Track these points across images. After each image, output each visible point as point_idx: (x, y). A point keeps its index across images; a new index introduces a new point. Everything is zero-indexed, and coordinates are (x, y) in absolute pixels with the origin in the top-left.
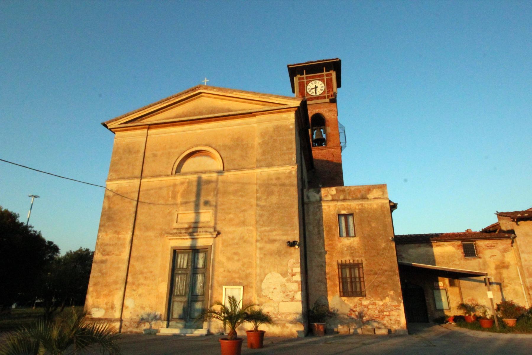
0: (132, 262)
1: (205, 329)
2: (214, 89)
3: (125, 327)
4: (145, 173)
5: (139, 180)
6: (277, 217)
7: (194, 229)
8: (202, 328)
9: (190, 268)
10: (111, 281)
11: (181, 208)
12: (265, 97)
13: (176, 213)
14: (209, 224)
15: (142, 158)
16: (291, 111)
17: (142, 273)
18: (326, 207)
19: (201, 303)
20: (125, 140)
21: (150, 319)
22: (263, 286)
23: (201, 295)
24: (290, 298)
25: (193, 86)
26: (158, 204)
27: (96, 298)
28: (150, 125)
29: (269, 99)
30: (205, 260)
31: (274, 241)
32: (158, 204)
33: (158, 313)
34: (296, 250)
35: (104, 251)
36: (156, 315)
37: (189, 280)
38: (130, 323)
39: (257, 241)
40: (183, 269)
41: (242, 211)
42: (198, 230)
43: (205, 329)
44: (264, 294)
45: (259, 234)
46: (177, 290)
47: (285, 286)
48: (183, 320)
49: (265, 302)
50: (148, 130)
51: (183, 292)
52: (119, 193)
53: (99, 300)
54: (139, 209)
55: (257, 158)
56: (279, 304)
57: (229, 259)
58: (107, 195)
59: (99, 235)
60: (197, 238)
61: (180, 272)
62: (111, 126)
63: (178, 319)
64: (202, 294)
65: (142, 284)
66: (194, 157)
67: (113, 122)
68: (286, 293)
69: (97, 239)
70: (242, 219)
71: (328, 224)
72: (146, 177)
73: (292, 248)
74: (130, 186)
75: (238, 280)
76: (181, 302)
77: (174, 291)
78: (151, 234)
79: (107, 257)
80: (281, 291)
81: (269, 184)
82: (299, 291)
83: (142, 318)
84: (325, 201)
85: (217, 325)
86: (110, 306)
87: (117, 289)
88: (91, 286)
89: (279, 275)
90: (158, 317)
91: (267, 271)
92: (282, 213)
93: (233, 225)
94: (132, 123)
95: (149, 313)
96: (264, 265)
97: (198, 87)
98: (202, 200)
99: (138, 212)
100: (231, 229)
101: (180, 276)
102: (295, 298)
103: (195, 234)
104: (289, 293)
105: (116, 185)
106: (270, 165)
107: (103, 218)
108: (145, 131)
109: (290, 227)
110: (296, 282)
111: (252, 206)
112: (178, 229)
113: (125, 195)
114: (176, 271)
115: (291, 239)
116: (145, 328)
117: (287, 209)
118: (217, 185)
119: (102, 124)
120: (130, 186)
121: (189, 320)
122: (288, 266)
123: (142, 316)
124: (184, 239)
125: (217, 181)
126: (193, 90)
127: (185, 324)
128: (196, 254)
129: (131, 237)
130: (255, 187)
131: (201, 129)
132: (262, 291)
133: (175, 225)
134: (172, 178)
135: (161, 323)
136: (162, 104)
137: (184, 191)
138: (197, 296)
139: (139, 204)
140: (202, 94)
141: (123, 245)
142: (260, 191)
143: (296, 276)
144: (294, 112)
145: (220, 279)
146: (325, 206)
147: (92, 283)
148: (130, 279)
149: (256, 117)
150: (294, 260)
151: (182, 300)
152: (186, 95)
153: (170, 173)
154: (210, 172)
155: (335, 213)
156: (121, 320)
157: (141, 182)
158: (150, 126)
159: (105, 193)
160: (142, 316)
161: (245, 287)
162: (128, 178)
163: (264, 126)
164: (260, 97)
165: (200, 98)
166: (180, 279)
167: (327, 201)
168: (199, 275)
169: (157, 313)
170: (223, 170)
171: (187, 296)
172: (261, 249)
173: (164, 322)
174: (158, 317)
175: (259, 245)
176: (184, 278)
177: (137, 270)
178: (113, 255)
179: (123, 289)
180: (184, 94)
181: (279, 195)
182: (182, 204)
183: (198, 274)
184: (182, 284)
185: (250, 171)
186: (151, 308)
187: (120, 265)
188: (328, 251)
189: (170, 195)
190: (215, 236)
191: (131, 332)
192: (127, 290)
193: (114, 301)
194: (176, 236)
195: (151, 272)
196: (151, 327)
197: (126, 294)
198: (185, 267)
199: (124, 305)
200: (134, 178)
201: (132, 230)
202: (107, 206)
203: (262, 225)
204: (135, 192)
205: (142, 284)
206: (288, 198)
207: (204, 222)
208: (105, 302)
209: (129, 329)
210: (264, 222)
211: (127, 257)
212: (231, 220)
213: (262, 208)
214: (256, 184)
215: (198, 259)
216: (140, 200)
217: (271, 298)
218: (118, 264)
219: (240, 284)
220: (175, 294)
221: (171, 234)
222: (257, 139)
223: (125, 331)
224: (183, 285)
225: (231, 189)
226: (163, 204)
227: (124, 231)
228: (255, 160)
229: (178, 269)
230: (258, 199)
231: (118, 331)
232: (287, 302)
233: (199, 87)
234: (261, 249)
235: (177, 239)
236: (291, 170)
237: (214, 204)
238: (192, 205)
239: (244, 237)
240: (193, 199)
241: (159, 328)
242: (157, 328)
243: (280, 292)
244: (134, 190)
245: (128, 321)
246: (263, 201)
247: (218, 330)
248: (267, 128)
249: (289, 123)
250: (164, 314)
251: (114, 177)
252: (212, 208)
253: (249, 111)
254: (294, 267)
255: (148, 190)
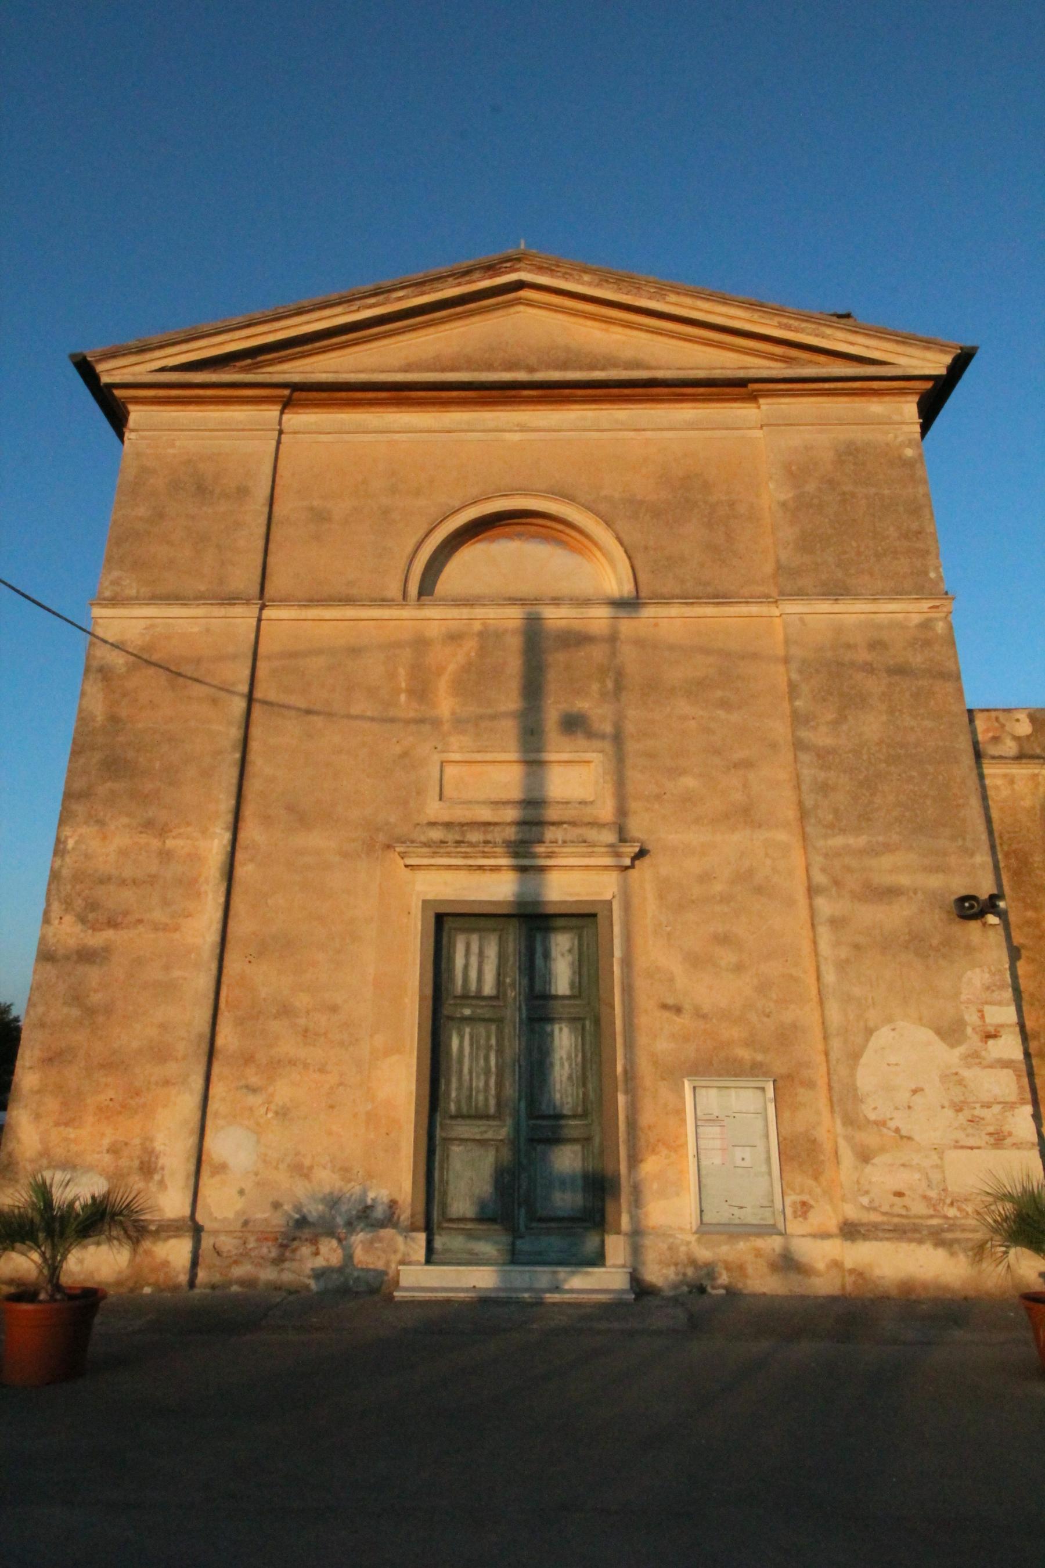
0: (234, 964)
1: (614, 1266)
2: (585, 272)
3: (217, 1261)
4: (277, 584)
5: (254, 610)
6: (891, 798)
7: (526, 828)
8: (598, 1259)
9: (511, 994)
10: (135, 1044)
11: (454, 740)
12: (804, 325)
13: (436, 758)
14: (588, 810)
15: (263, 520)
16: (902, 392)
17: (286, 1011)
18: (999, 782)
19: (577, 1148)
20: (178, 443)
21: (340, 1221)
22: (866, 1079)
23: (574, 1116)
24: (990, 1134)
25: (492, 255)
26: (350, 717)
27: (57, 1124)
28: (296, 387)
29: (823, 336)
30: (580, 961)
31: (889, 893)
32: (350, 717)
33: (379, 1194)
34: (991, 933)
35: (93, 906)
36: (369, 1202)
37: (513, 1046)
38: (241, 1241)
39: (812, 891)
40: (479, 996)
41: (735, 766)
42: (543, 834)
43: (614, 1266)
44: (872, 1116)
45: (818, 860)
46: (459, 1089)
47: (961, 1082)
48: (496, 1227)
49: (883, 1149)
50: (282, 412)
51: (486, 1099)
52: (155, 658)
53: (71, 1133)
54: (255, 732)
55: (778, 561)
56: (941, 1158)
57: (696, 961)
58: (95, 664)
59: (67, 838)
60: (542, 869)
61: (467, 1012)
62: (114, 372)
63: (472, 1220)
64: (580, 1110)
65: (292, 1063)
66: (492, 540)
67: (124, 355)
68: (967, 1114)
69: (56, 853)
70: (738, 797)
71: (1014, 846)
72: (285, 601)
73: (974, 925)
74: (208, 630)
75: (744, 1054)
76: (482, 1143)
77: (448, 1093)
78: (316, 839)
79: (110, 934)
80: (946, 1104)
81: (840, 664)
82: (1023, 1102)
83: (297, 1216)
84: (993, 758)
85: (670, 1248)
86: (136, 1163)
87: (167, 1083)
88: (31, 1068)
89: (930, 1035)
90: (379, 1213)
91: (872, 1016)
92: (910, 779)
93: (697, 820)
94: (215, 371)
95: (331, 1193)
96: (857, 991)
97: (514, 261)
98: (552, 714)
99: (254, 745)
100: (695, 837)
101: (468, 1030)
102: (1010, 1134)
103: (540, 849)
104: (978, 1112)
105: (143, 623)
106: (836, 591)
107: (82, 761)
108: (271, 413)
109: (953, 838)
110: (1006, 1064)
111: (774, 746)
112: (448, 825)
113: (187, 669)
114: (447, 1011)
115: (960, 886)
116: (319, 1262)
117: (930, 769)
118: (614, 654)
119: (72, 357)
120: (208, 630)
121: (527, 1228)
122: (963, 997)
123: (298, 1208)
124: (480, 868)
125: (613, 638)
126: (491, 269)
127: (513, 1244)
128: (539, 938)
129: (229, 849)
130: (780, 676)
131: (523, 429)
132: (861, 1101)
133: (434, 810)
134: (405, 613)
135: (400, 1239)
136: (355, 308)
137: (467, 668)
138: (560, 1117)
139: (257, 711)
140: (524, 293)
141: (190, 885)
142: (805, 689)
143: (1001, 1041)
144: (916, 398)
145: (663, 1046)
146: (994, 776)
147: (37, 1053)
148: (226, 1037)
149: (762, 401)
150: (987, 975)
151: (486, 1136)
152: (459, 285)
153: (394, 589)
154: (585, 602)
155: (1038, 807)
156: (197, 1231)
157: (259, 620)
158: (297, 395)
159: (89, 657)
160: (298, 1208)
161: (780, 1083)
162: (200, 598)
163: (795, 439)
164: (781, 326)
165: (512, 310)
166: (471, 1045)
167: (1001, 757)
168: (556, 1027)
169: (371, 1195)
170: (634, 594)
171: (509, 1121)
172: (837, 923)
173: (414, 1234)
174: (379, 1213)
175: (825, 906)
176: (488, 1038)
177: (265, 1000)
178: (141, 928)
179: (197, 1082)
180: (450, 279)
181: (891, 711)
182: (459, 723)
183: (550, 1020)
184: (482, 1062)
185: (754, 609)
186: (345, 1171)
187: (176, 973)
188: (1024, 946)
189: (403, 685)
190: (627, 862)
191: (249, 1283)
192: (217, 1089)
193: (152, 1140)
194: (449, 855)
195: (334, 1009)
196: (349, 1257)
197: (212, 1106)
198: (488, 989)
199: (204, 1158)
200: (231, 599)
201: (230, 818)
202: (98, 708)
203: (831, 826)
204: (234, 657)
205: (292, 1063)
206: (928, 724)
207: (567, 803)
208: (106, 1142)
209: (239, 1271)
210: (836, 811)
211: (212, 937)
212: (687, 799)
213: (823, 756)
214: (786, 660)
215: (547, 955)
216: (258, 694)
217: (904, 1133)
218: (167, 968)
219: (756, 1070)
220: (453, 1107)
221: (425, 845)
222: (772, 486)
223: (217, 1278)
224: (487, 1072)
225: (676, 675)
226: (372, 719)
227: (188, 824)
228: (769, 568)
229: (456, 997)
230: (798, 719)
231: (183, 1278)
232: (979, 1148)
233: (519, 260)
234: (837, 923)
235: (449, 867)
236: (926, 616)
237: (608, 728)
238: (509, 728)
239: (750, 872)
240: (510, 701)
241: (388, 1263)
242: (380, 1265)
243: (943, 1107)
244: (231, 649)
245: (229, 1233)
246: (823, 729)
247: (677, 1274)
248: (807, 448)
249: (900, 439)
250: (409, 1199)
251: (133, 592)
252: (597, 744)
253: (742, 374)
254: (987, 1003)
255: (293, 655)
